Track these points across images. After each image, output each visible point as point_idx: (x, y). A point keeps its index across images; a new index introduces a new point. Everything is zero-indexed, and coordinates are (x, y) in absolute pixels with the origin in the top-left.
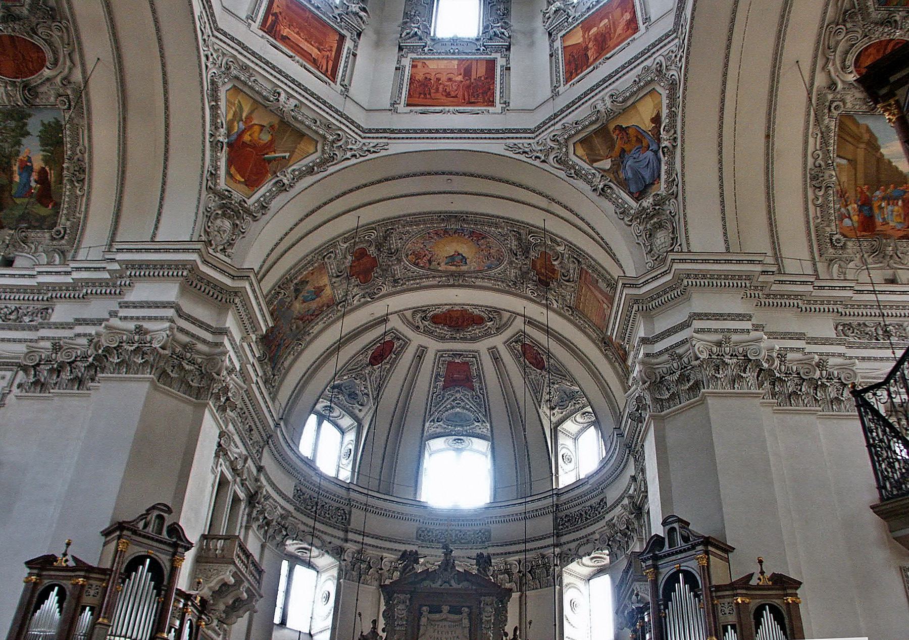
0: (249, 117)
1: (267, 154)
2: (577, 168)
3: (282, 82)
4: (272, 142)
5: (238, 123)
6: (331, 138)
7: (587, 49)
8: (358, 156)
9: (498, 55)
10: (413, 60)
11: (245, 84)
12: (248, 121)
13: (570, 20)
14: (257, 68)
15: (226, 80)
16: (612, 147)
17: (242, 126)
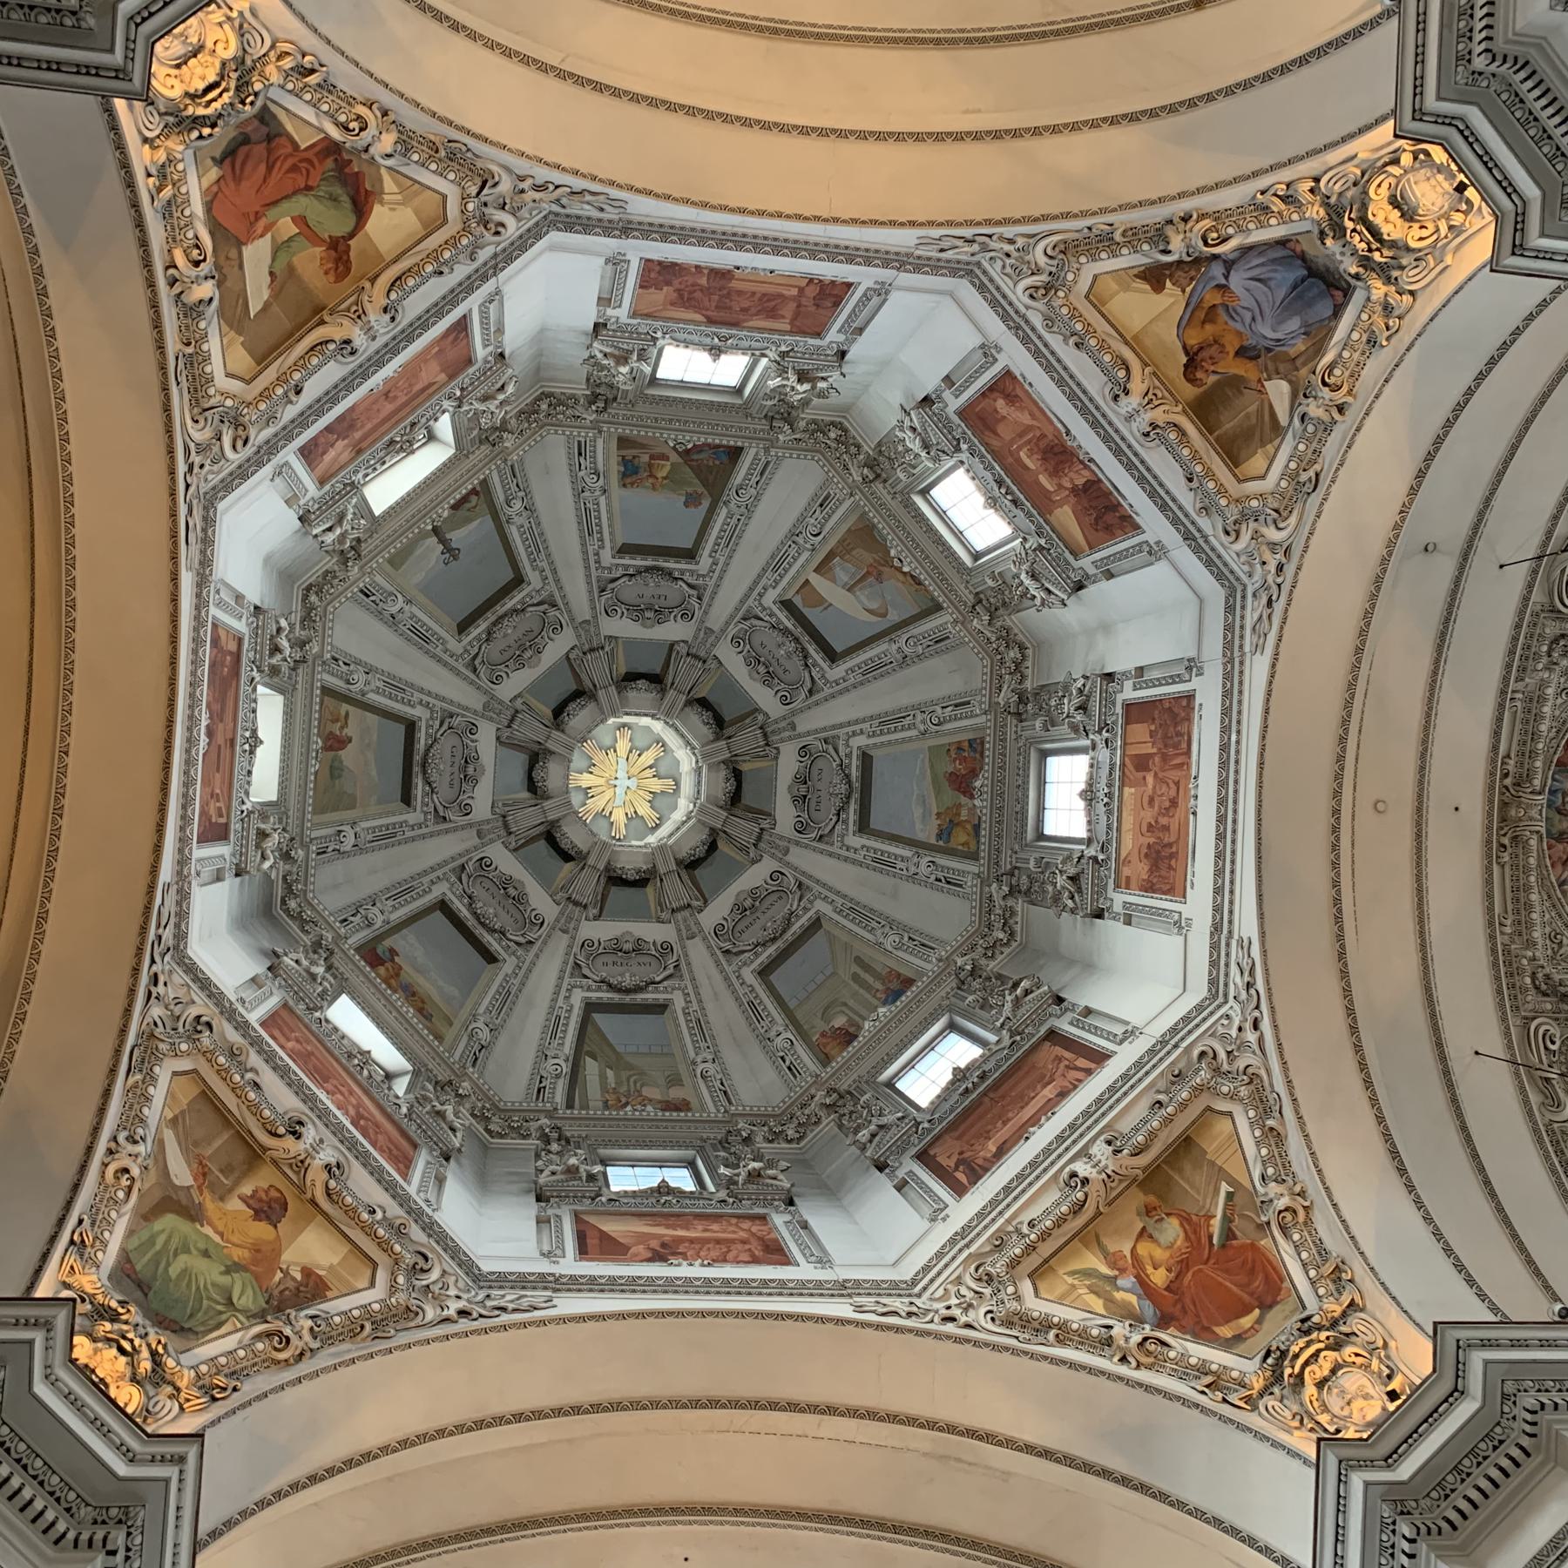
0: (1113, 1260)
1: (1210, 1237)
2: (1293, 465)
3: (1052, 1163)
4: (1185, 1219)
5: (1118, 1289)
6: (1204, 1075)
7: (1074, 490)
8: (1256, 1013)
9: (1120, 698)
10: (1117, 886)
11: (1031, 1249)
12: (1121, 1264)
13: (1043, 542)
14: (1007, 1215)
15: (1011, 1290)
16: (1235, 384)
17: (1127, 1281)
